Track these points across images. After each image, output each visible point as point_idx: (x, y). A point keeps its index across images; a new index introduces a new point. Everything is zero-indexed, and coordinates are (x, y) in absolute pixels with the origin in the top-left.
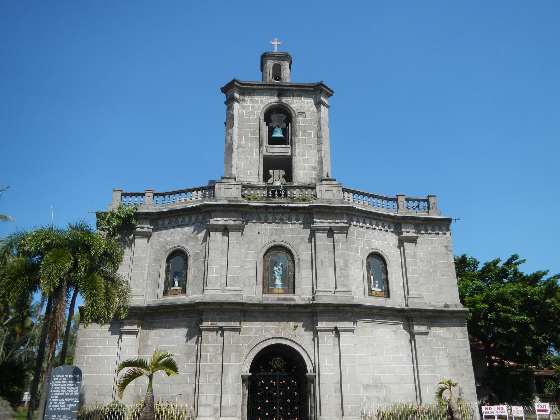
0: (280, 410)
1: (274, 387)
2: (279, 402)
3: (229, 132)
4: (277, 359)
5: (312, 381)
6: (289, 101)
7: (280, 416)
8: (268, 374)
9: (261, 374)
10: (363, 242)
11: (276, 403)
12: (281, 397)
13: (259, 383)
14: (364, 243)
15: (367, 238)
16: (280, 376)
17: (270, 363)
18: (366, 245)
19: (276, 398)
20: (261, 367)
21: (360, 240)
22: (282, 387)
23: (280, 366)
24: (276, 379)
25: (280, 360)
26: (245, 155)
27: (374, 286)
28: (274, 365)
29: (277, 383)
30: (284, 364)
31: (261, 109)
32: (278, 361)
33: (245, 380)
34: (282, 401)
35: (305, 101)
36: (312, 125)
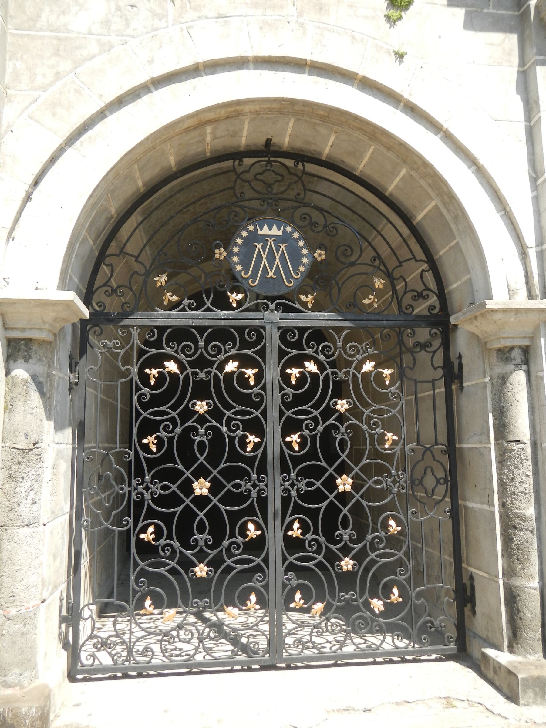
0: (288, 540)
1: (245, 400)
2: (279, 492)
4: (265, 231)
5: (517, 354)
7: (293, 579)
8: (206, 323)
9: (159, 323)
11: (263, 502)
12: (296, 461)
13: (144, 378)
16: (284, 332)
19: (262, 470)
20: (162, 279)
22: (299, 400)
24: (262, 353)
25: (285, 238)
28: (246, 268)
29: (268, 377)
32: (270, 241)
33: (29, 341)
34: (302, 485)
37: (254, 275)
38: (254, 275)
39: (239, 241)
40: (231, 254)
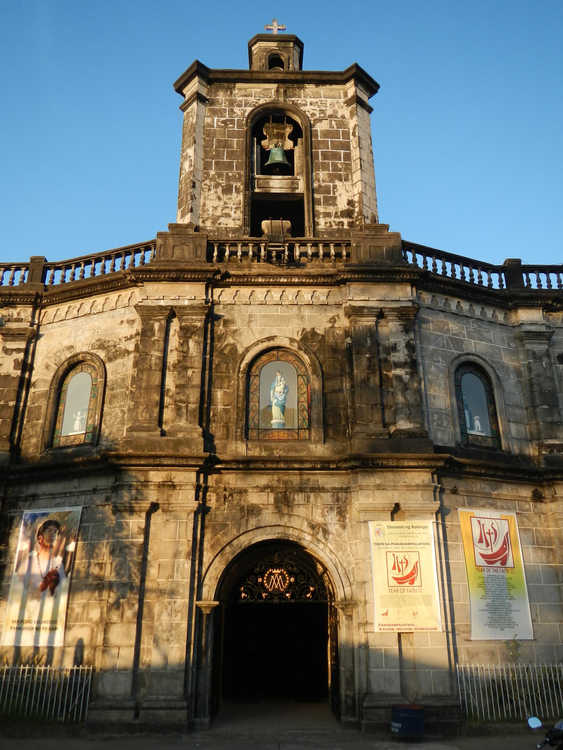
3: (186, 155)
6: (297, 101)
10: (447, 340)
14: (447, 343)
15: (454, 334)
17: (260, 580)
18: (451, 346)
21: (440, 336)
23: (282, 587)
25: (281, 574)
26: (216, 192)
27: (472, 428)
28: (268, 585)
30: (290, 583)
31: (246, 114)
32: (277, 575)
35: (326, 101)
36: (341, 139)
37: (271, 587)
38: (271, 587)
39: (266, 575)
40: (263, 579)
